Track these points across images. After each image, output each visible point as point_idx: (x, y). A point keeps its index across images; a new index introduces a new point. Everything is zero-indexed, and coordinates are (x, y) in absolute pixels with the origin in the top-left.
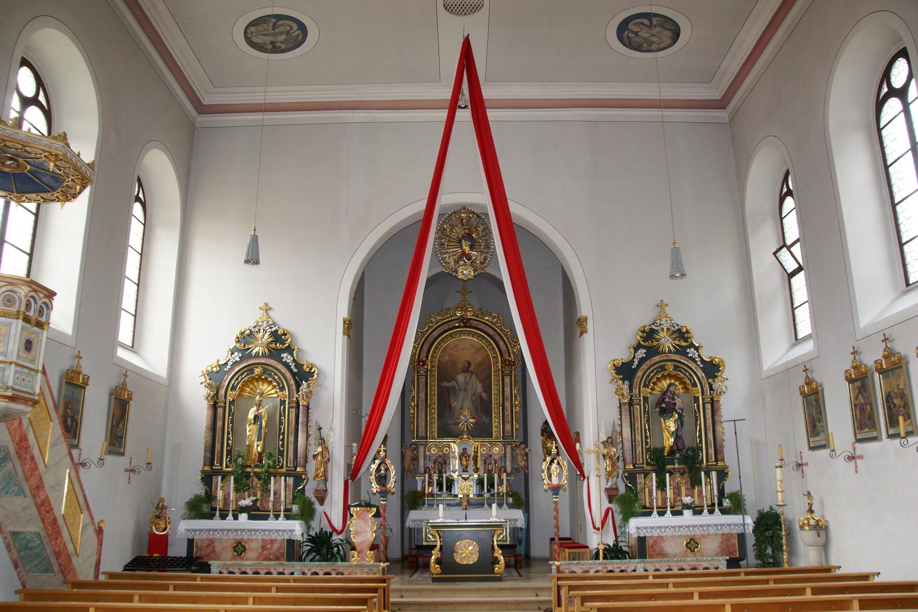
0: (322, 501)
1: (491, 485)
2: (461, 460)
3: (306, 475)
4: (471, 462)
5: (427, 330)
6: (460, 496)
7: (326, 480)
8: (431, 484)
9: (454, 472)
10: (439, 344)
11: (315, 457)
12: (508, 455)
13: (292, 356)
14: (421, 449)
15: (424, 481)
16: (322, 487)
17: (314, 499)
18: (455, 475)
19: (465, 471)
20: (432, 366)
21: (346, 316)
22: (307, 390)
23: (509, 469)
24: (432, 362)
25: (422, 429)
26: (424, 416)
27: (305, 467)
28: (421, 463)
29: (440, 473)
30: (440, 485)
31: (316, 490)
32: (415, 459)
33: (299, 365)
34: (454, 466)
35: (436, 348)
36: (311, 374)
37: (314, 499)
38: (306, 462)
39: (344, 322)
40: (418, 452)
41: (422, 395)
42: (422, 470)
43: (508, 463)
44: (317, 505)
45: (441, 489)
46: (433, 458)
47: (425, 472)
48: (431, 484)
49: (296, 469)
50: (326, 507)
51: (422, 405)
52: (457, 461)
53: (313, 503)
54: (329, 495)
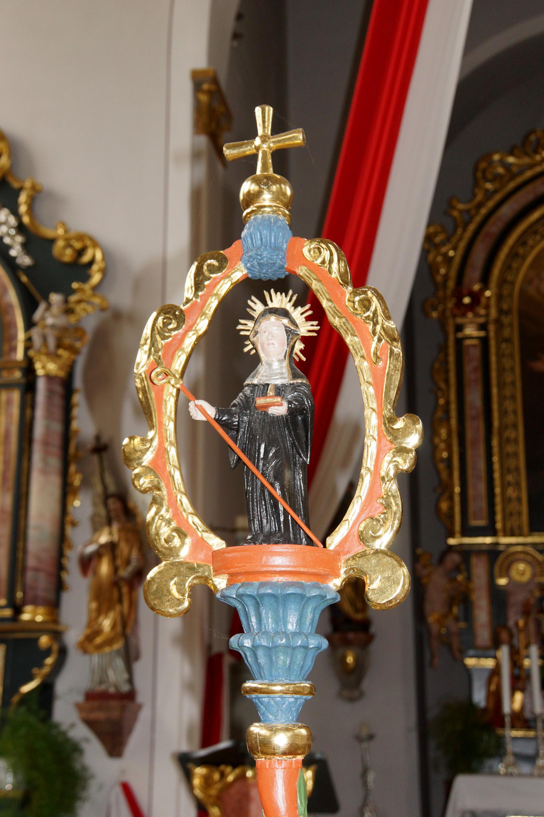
0: (114, 740)
3: (57, 635)
5: (480, 205)
7: (130, 656)
8: (520, 681)
10: (522, 241)
11: (87, 564)
13: (14, 211)
14: (479, 568)
16: (116, 676)
17: (80, 732)
20: (501, 311)
21: (201, 62)
22: (62, 321)
24: (500, 297)
25: (477, 504)
26: (482, 465)
27: (54, 605)
28: (482, 615)
31: (90, 696)
32: (463, 600)
33: (35, 242)
35: (513, 255)
36: (79, 270)
37: (80, 732)
38: (60, 586)
39: (197, 86)
40: (469, 578)
41: (474, 398)
42: (483, 635)
44: (94, 755)
47: (496, 644)
49: (18, 610)
50: (131, 765)
51: (475, 429)
53: (76, 749)
54: (144, 715)
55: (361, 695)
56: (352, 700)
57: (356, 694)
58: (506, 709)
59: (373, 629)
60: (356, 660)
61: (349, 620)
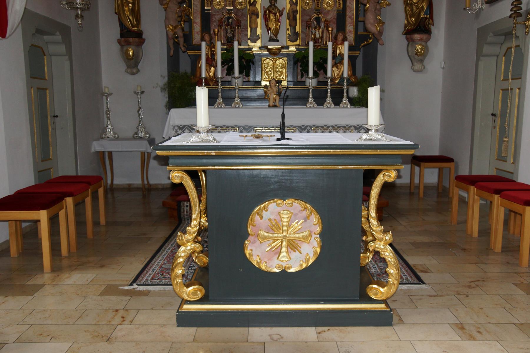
1: (321, 65)
2: (266, 19)
4: (285, 23)
6: (264, 83)
8: (211, 61)
9: (255, 41)
12: (351, 13)
15: (199, 57)
18: (255, 47)
19: (274, 39)
23: (351, 37)
29: (230, 41)
30: (228, 62)
34: (254, 30)
43: (350, 28)
45: (230, 71)
46: (217, 17)
48: (211, 61)
52: (260, 21)
55: (138, 71)
56: (133, 74)
57: (135, 71)
58: (203, 75)
59: (144, 37)
60: (133, 53)
61: (129, 31)
